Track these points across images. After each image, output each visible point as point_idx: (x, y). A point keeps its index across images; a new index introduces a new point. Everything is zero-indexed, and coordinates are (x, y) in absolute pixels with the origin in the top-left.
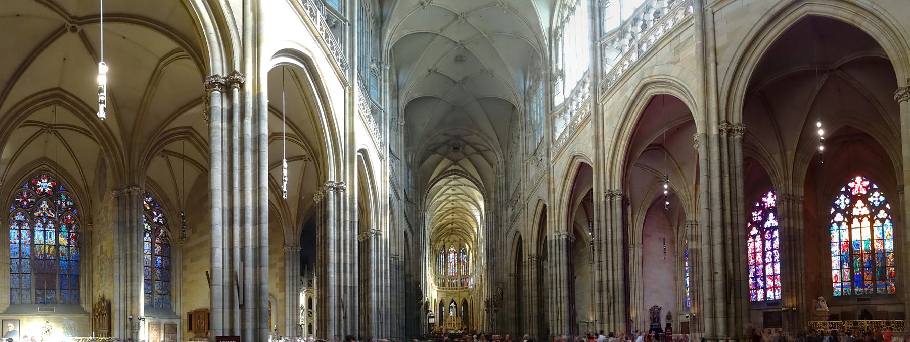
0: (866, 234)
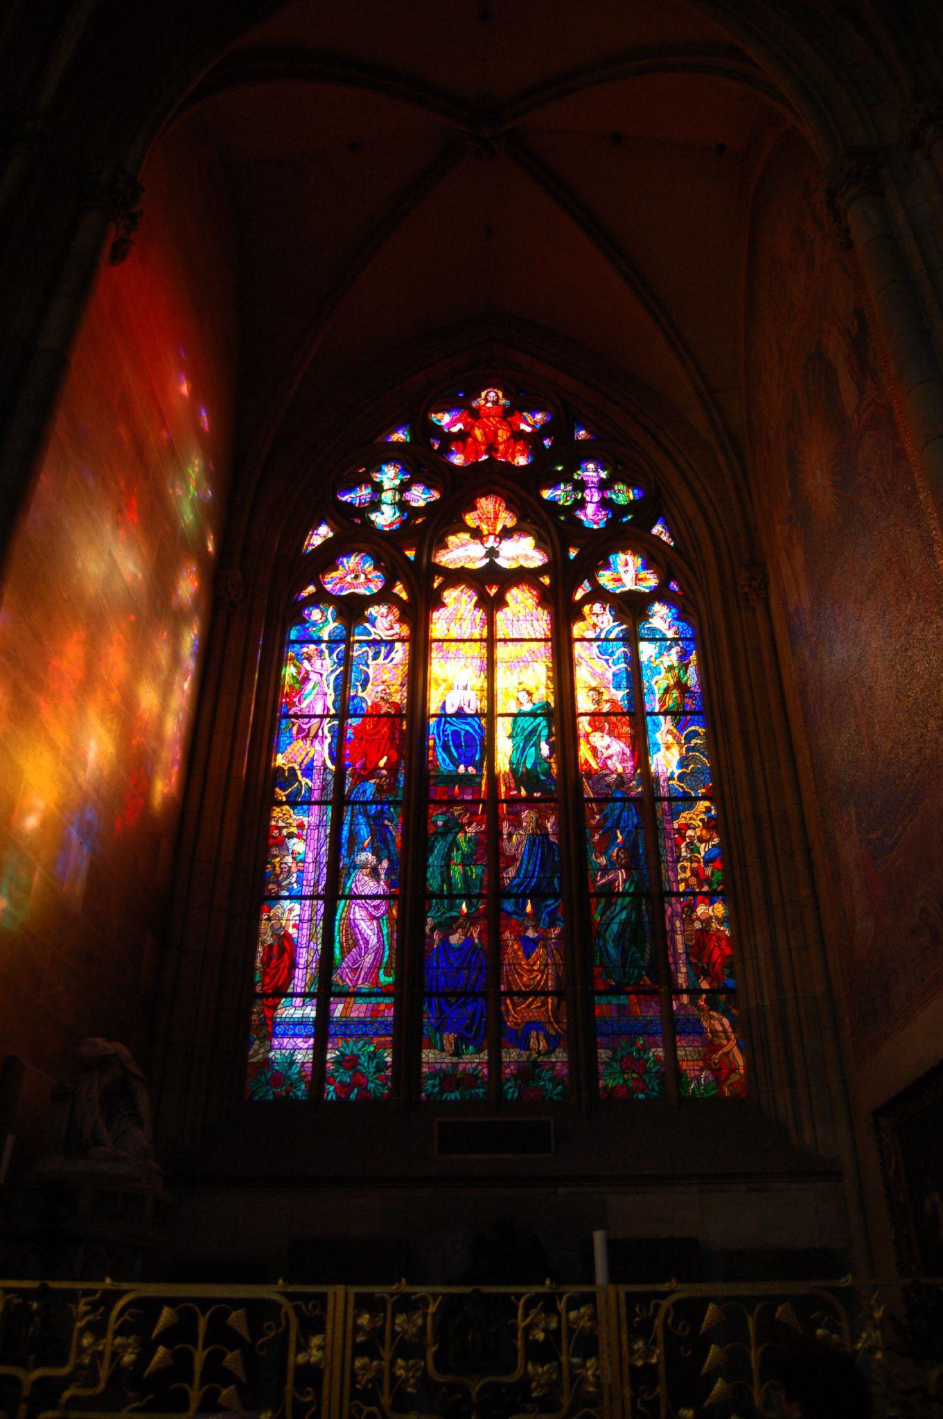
0: (525, 680)
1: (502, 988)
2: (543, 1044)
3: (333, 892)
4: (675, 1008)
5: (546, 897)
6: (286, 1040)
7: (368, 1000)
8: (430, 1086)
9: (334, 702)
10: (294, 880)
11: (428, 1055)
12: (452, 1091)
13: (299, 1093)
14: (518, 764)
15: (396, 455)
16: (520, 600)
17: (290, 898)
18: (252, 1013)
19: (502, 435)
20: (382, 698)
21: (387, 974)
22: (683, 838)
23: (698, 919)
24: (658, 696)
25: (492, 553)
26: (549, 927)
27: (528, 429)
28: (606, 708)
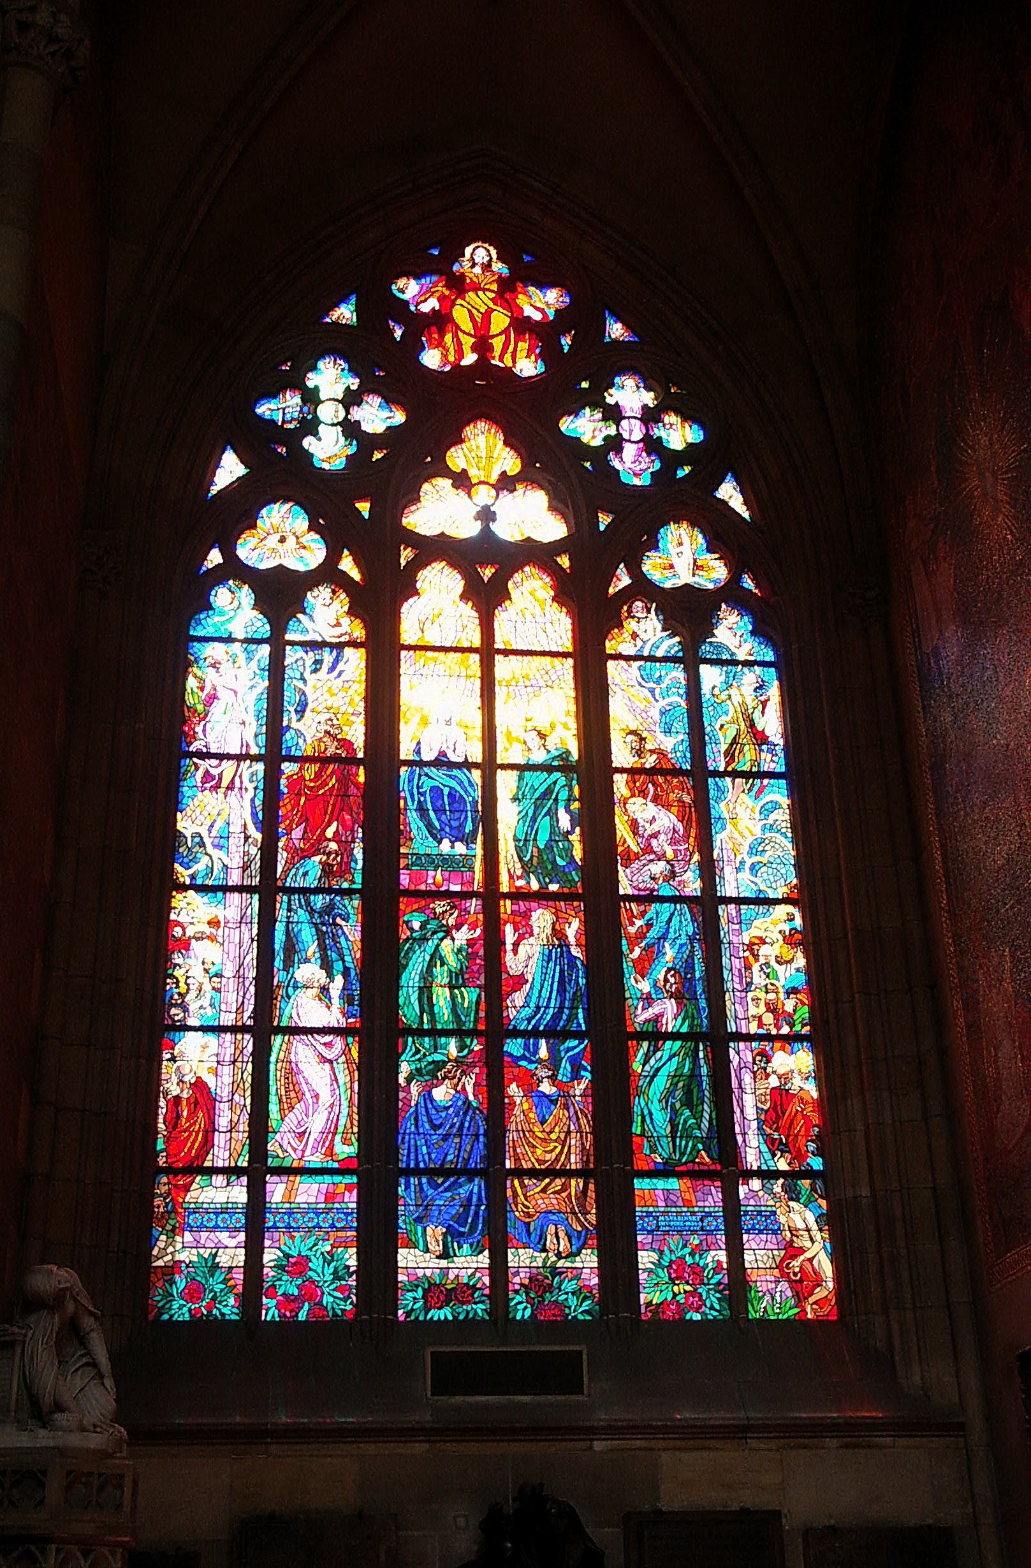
0: (540, 712)
1: (508, 1164)
2: (564, 1244)
3: (263, 1025)
4: (742, 1196)
5: (567, 1035)
6: (204, 1235)
7: (319, 1179)
8: (410, 1302)
9: (256, 736)
10: (206, 1003)
11: (406, 1257)
12: (440, 1308)
13: (225, 1310)
14: (525, 840)
15: (339, 344)
16: (531, 590)
17: (204, 1029)
18: (153, 1196)
19: (500, 321)
20: (327, 732)
21: (346, 1141)
22: (756, 957)
23: (774, 1072)
24: (723, 748)
25: (486, 515)
26: (572, 1080)
27: (537, 316)
28: (650, 761)
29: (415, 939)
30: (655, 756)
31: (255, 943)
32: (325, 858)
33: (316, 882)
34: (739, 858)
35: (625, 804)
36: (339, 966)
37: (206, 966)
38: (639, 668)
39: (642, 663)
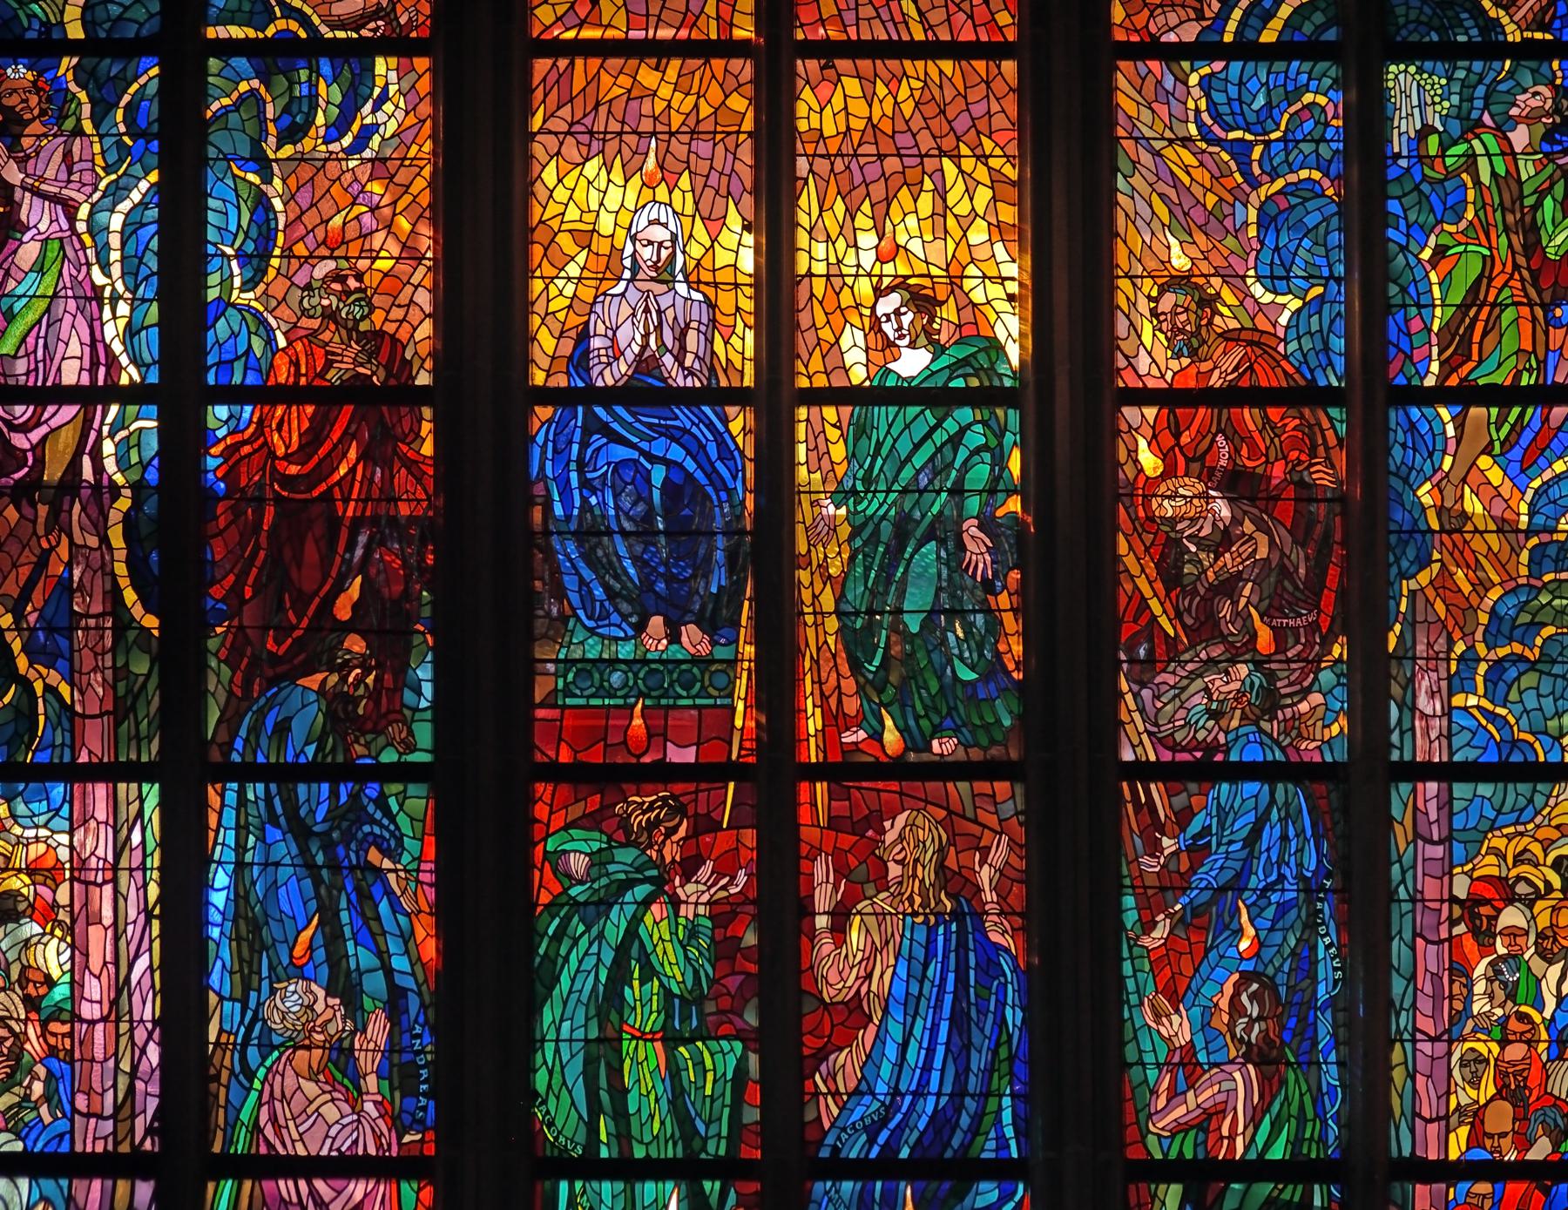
20: (330, 315)
28: (1223, 369)
29: (575, 904)
30: (1238, 353)
31: (156, 924)
32: (334, 678)
33: (311, 750)
34: (1460, 648)
35: (1147, 498)
36: (375, 983)
37: (31, 990)
38: (1206, 84)
39: (1218, 66)
